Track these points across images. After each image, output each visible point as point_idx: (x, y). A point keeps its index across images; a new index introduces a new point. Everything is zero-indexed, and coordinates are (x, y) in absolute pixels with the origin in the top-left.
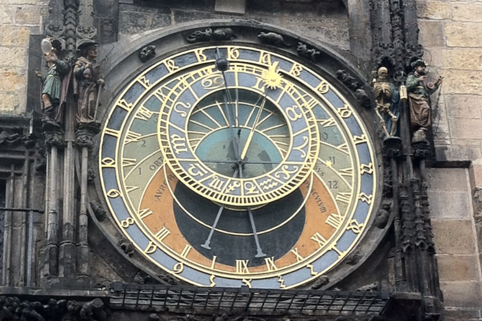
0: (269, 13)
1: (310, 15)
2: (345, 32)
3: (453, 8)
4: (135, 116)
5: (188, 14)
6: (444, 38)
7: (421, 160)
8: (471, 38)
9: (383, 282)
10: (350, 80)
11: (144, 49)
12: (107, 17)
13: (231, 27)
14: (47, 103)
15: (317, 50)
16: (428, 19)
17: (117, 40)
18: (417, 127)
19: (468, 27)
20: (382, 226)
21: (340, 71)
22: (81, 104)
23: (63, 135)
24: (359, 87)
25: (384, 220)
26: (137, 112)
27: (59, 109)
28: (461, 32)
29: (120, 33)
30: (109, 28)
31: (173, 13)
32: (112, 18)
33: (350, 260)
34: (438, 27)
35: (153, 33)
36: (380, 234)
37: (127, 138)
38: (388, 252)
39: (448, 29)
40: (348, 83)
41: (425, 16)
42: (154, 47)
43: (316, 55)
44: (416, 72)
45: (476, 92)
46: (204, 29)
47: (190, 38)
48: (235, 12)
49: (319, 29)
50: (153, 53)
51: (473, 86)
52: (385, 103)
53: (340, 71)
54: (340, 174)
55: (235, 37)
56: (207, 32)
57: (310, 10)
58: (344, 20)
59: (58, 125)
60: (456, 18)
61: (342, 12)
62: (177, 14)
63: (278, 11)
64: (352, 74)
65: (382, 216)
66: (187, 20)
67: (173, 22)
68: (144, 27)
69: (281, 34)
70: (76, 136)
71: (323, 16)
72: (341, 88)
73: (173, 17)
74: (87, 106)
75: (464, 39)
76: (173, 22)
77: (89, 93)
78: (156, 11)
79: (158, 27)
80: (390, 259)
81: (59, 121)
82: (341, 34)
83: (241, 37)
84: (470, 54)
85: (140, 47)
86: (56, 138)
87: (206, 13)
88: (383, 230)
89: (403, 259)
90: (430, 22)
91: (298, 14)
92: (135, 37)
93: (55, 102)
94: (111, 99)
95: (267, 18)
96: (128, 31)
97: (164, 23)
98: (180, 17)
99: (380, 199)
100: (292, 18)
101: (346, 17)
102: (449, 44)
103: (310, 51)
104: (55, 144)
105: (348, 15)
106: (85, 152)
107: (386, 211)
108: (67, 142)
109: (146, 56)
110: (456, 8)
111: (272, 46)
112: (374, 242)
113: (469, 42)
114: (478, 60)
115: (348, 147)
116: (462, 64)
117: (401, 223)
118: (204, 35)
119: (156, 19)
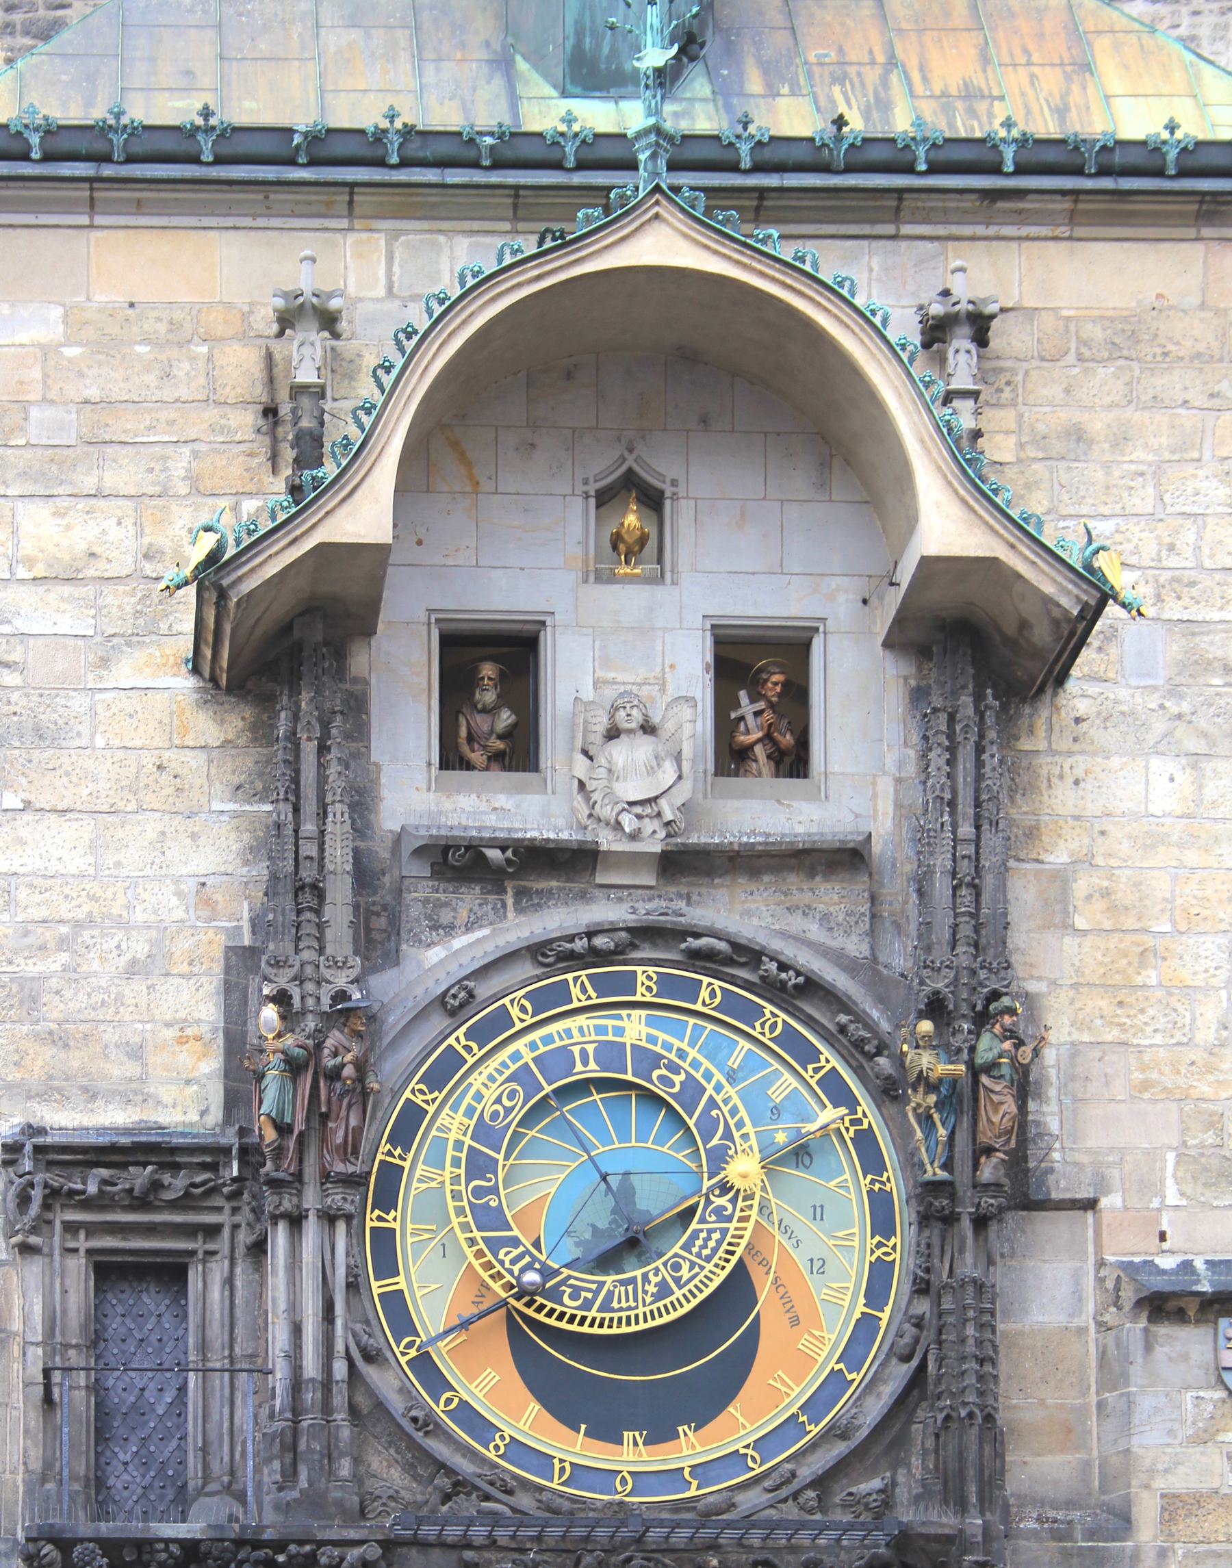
0: (706, 880)
1: (792, 879)
2: (863, 914)
3: (1096, 835)
4: (434, 1132)
5: (540, 893)
6: (1071, 909)
7: (991, 1218)
8: (1127, 909)
9: (900, 1471)
10: (863, 1040)
11: (452, 991)
12: (377, 898)
13: (628, 930)
14: (270, 1135)
15: (798, 974)
16: (1042, 862)
17: (397, 964)
18: (989, 1151)
19: (1124, 880)
20: (907, 1359)
21: (843, 1018)
22: (334, 1131)
23: (299, 1193)
24: (879, 1053)
25: (906, 1352)
26: (438, 1124)
27: (291, 1143)
28: (1106, 893)
29: (404, 947)
30: (381, 922)
31: (510, 893)
32: (388, 898)
33: (837, 1432)
34: (1061, 879)
35: (470, 945)
36: (901, 1372)
37: (419, 1181)
38: (915, 1410)
39: (1081, 886)
40: (859, 1044)
41: (1034, 856)
42: (471, 984)
43: (796, 986)
44: (998, 1026)
45: (1124, 1037)
46: (571, 939)
47: (545, 955)
48: (637, 882)
49: (807, 911)
50: (471, 995)
51: (1118, 1025)
52: (926, 1093)
53: (843, 1018)
54: (831, 1242)
55: (634, 946)
56: (580, 945)
57: (792, 869)
58: (861, 884)
59: (290, 1179)
60: (1099, 860)
61: (857, 869)
62: (520, 894)
63: (726, 873)
64: (867, 1026)
65: (907, 1339)
66: (538, 907)
67: (511, 914)
68: (452, 927)
69: (729, 941)
70: (324, 1193)
71: (818, 878)
72: (844, 1052)
73: (510, 901)
74: (346, 1141)
75: (1113, 909)
76: (511, 914)
77: (349, 1106)
78: (477, 889)
79: (481, 927)
80: (915, 1426)
81: (292, 1170)
82: (852, 920)
83: (646, 945)
84: (1121, 946)
85: (444, 988)
86: (287, 1205)
87: (576, 886)
88: (905, 1367)
89: (937, 1436)
90: (1043, 870)
91: (766, 878)
92: (435, 954)
93: (283, 1129)
94: (387, 1100)
95: (704, 890)
96: (420, 941)
97: (492, 916)
98: (527, 900)
99: (906, 1298)
100: (753, 887)
101: (866, 879)
102: (1080, 922)
103: (783, 976)
104: (284, 1216)
105: (871, 875)
106: (341, 1227)
107: (914, 1330)
108: (307, 1210)
109: (454, 1004)
110: (1103, 833)
111: (709, 965)
112: (889, 1391)
113: (1122, 918)
114: (1136, 960)
115: (850, 1184)
116: (1102, 971)
117: (940, 1361)
118: (572, 951)
119: (476, 908)
